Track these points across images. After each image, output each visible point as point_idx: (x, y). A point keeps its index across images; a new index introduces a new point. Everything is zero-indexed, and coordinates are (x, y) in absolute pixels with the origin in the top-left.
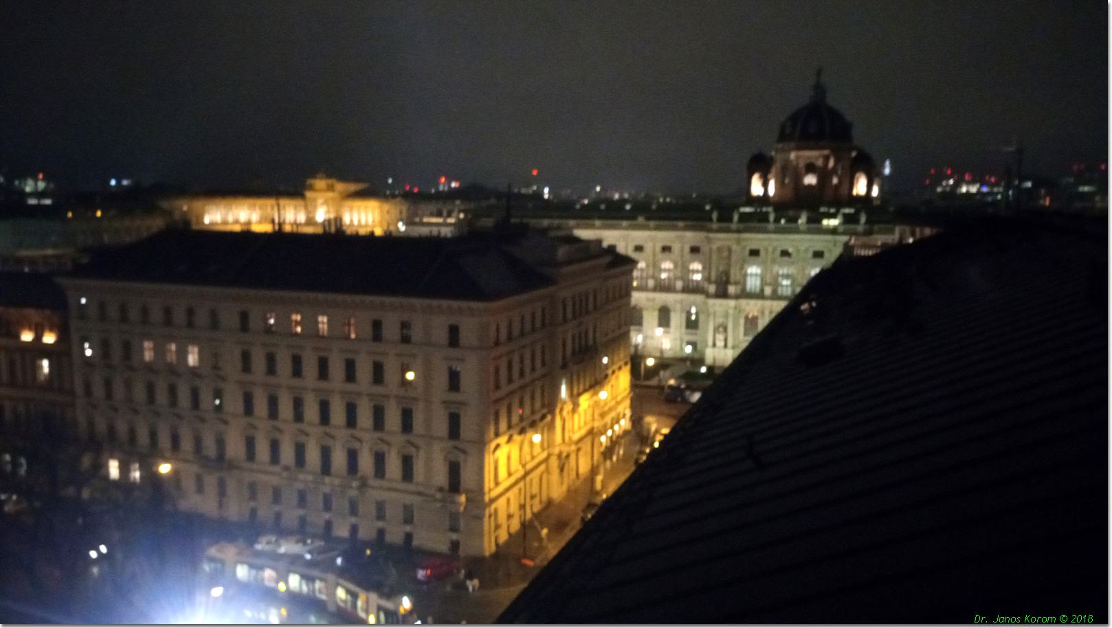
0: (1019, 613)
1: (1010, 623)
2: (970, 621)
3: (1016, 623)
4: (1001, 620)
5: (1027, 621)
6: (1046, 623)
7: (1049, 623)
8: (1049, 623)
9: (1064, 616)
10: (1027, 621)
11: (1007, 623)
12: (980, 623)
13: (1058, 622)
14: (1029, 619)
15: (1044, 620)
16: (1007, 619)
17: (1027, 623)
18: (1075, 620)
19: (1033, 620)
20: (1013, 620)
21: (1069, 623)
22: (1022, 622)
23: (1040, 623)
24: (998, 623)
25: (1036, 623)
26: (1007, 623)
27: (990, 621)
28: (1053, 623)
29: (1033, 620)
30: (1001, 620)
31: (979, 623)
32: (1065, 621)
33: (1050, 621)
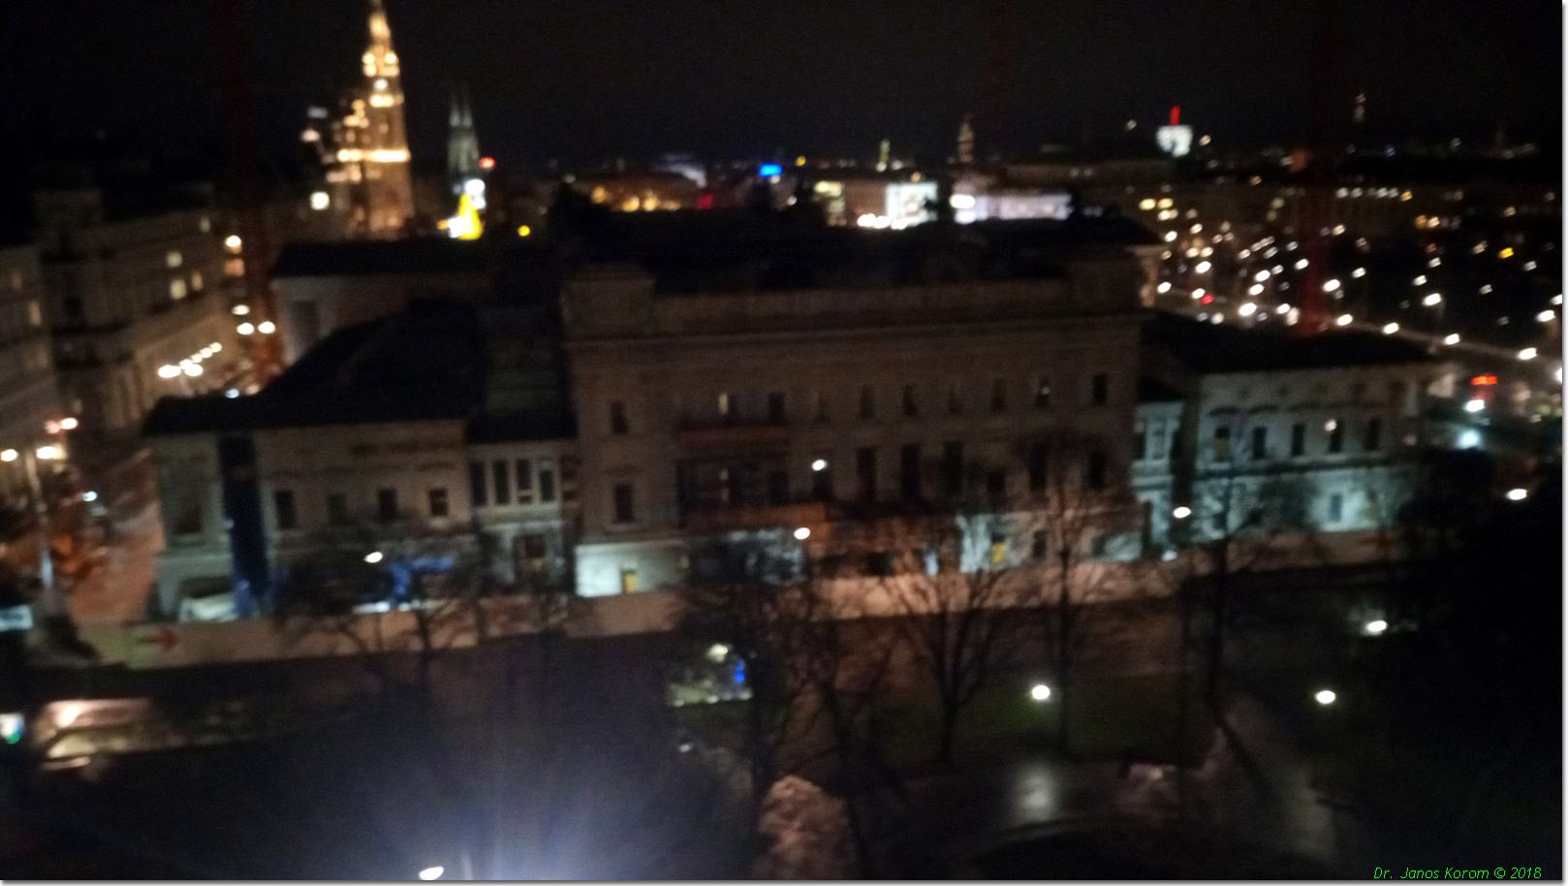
0: (1438, 866)
1: (1425, 879)
2: (1368, 877)
3: (1432, 879)
4: (1412, 874)
5: (1448, 876)
6: (1475, 879)
7: (1480, 879)
8: (1480, 879)
9: (1501, 869)
10: (1448, 876)
11: (1420, 879)
12: (1382, 879)
13: (1492, 878)
14: (1451, 873)
15: (1473, 874)
16: (1421, 873)
17: (1448, 878)
18: (1516, 875)
19: (1457, 874)
20: (1429, 874)
21: (1507, 878)
22: (1441, 878)
23: (1466, 879)
24: (1408, 879)
25: (1461, 879)
26: (1420, 879)
27: (1396, 876)
28: (1485, 879)
29: (1457, 874)
30: (1412, 874)
31: (1380, 879)
32: (1501, 877)
33: (1480, 876)
